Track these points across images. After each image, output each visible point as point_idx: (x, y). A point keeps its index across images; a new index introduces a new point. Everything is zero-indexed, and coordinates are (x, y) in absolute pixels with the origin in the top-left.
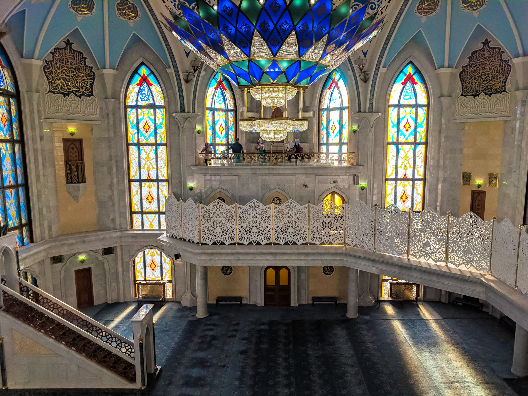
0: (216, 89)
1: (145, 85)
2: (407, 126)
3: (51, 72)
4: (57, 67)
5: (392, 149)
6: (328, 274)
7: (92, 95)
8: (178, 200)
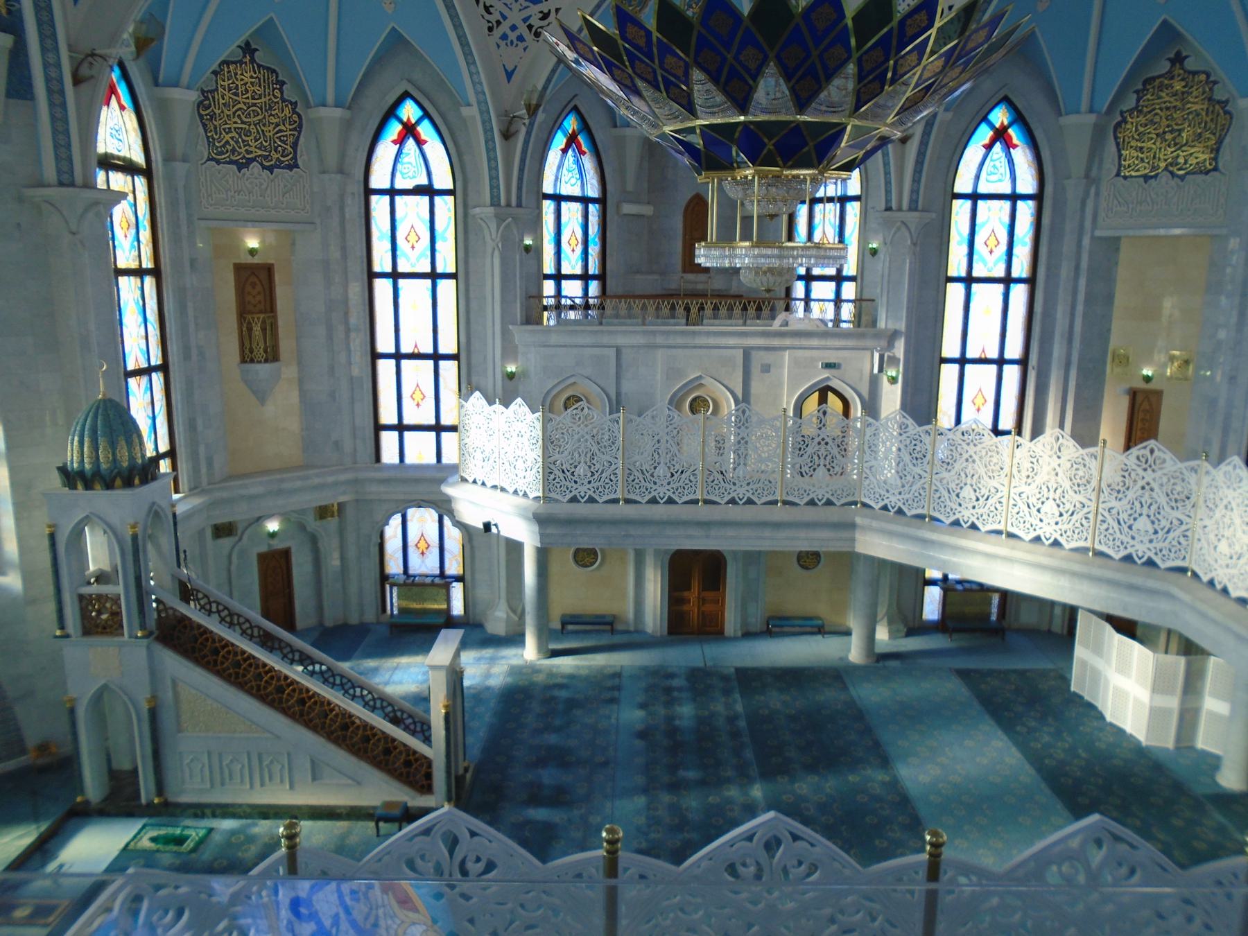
0: (565, 151)
1: (411, 142)
2: (992, 242)
3: (213, 116)
4: (224, 104)
5: (955, 292)
6: (807, 568)
7: (297, 166)
8: (491, 403)
